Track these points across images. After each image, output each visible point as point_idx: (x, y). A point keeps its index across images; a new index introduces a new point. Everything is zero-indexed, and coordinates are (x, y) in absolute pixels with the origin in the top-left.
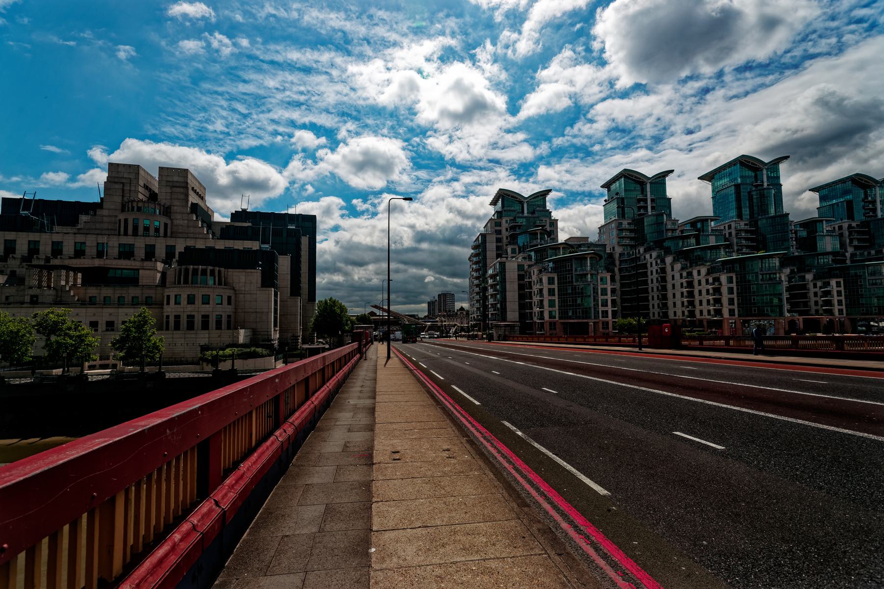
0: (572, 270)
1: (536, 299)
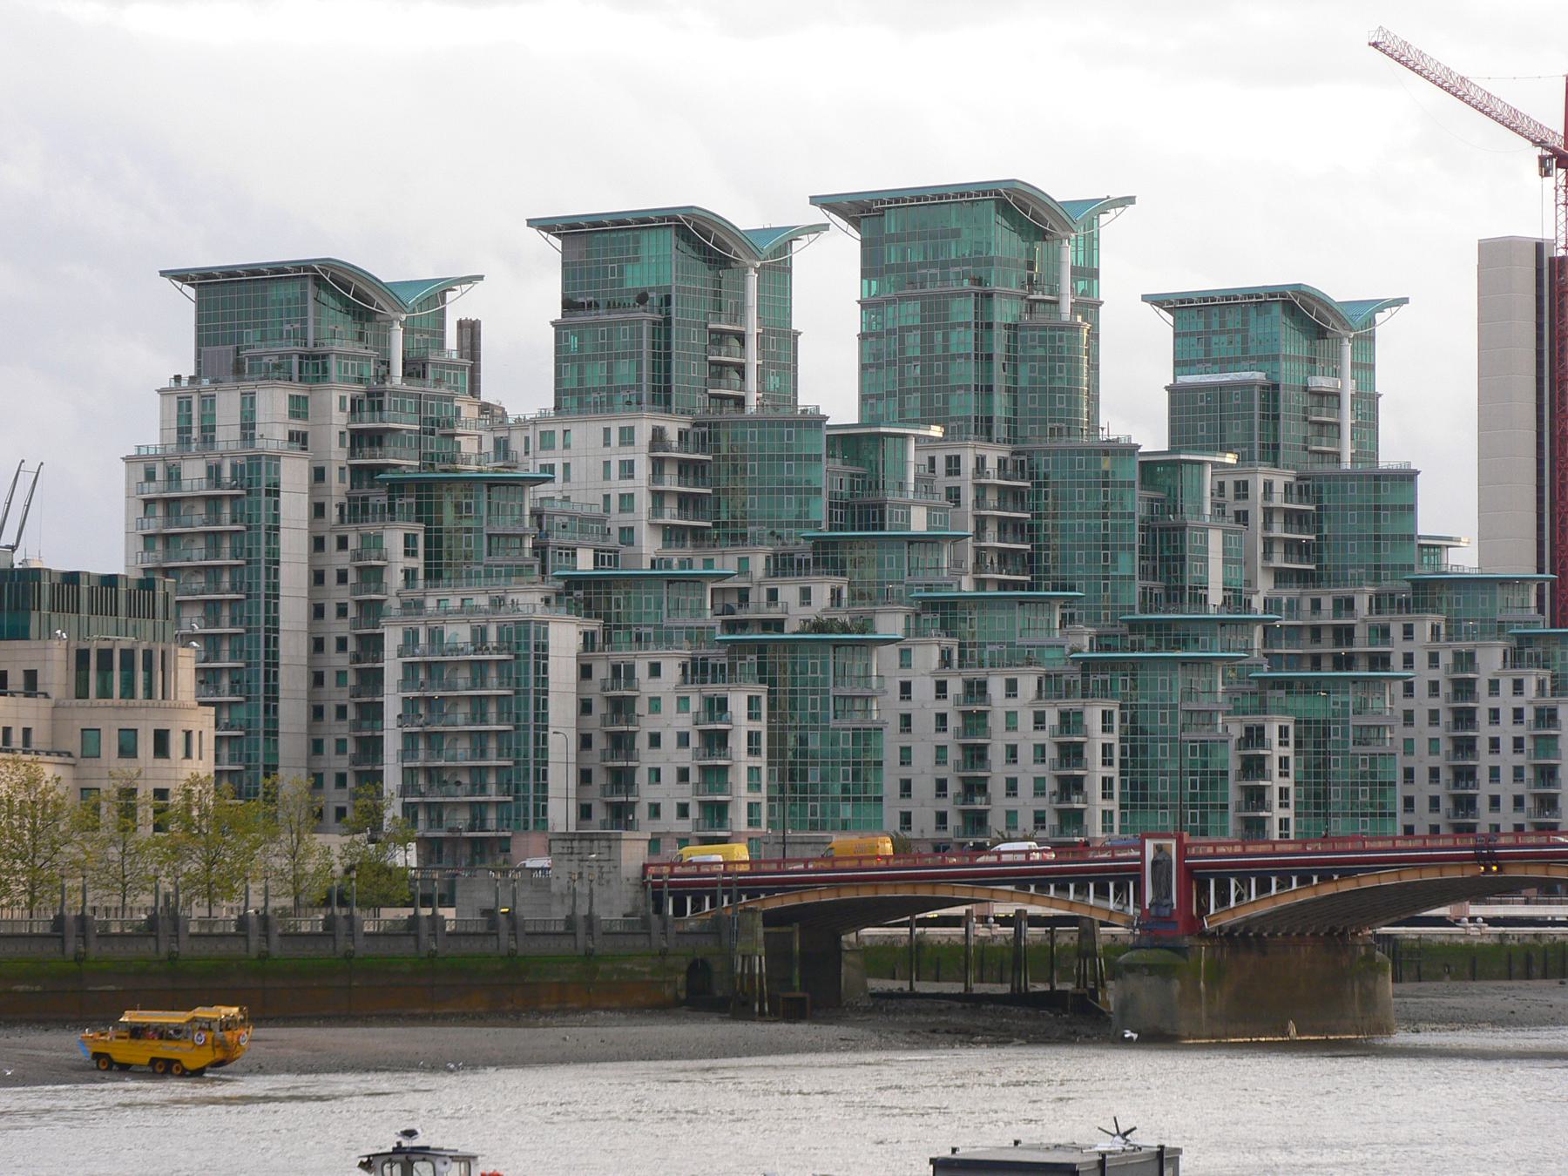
0: (825, 682)
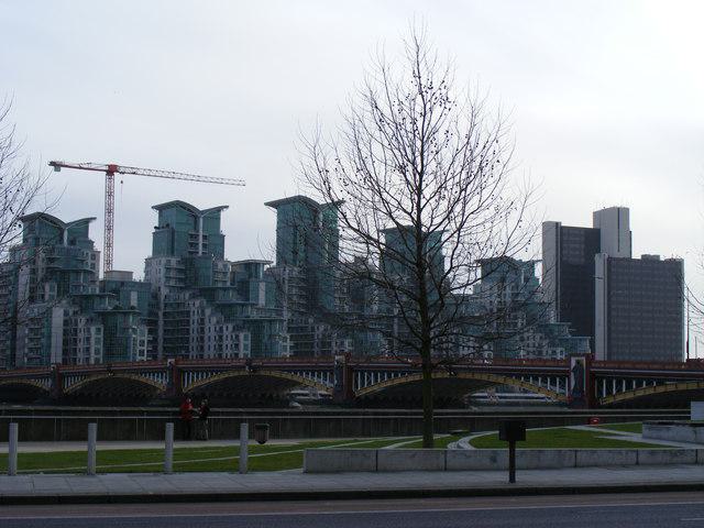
1: (81, 345)
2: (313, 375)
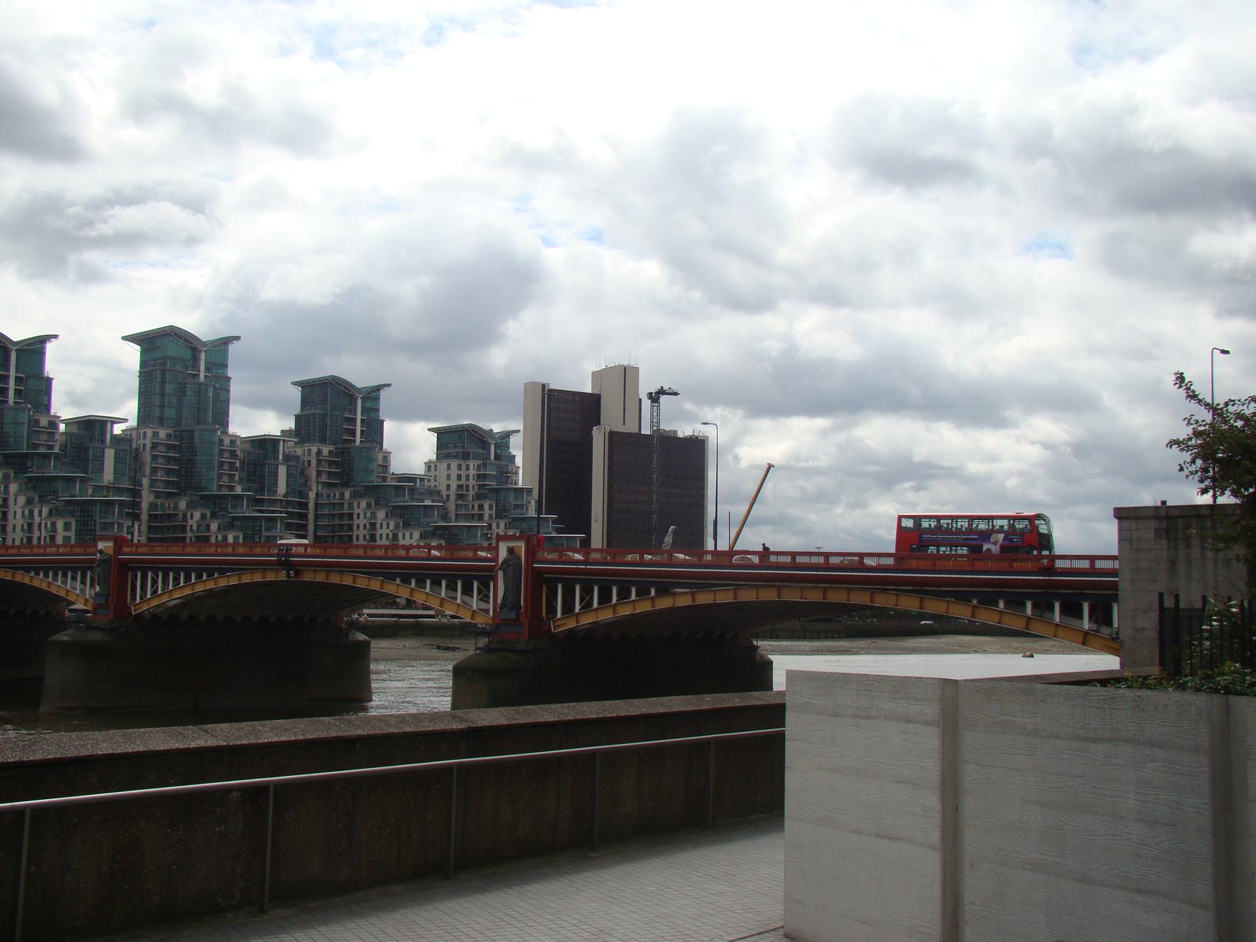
2: (65, 575)
